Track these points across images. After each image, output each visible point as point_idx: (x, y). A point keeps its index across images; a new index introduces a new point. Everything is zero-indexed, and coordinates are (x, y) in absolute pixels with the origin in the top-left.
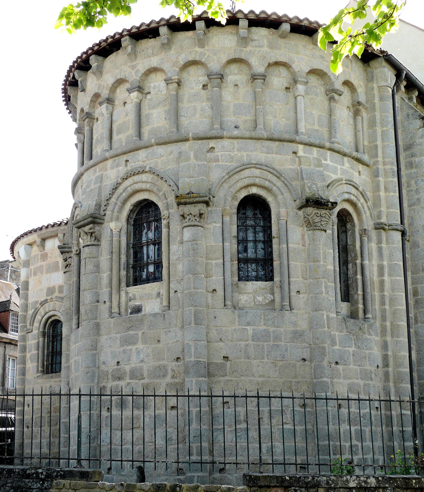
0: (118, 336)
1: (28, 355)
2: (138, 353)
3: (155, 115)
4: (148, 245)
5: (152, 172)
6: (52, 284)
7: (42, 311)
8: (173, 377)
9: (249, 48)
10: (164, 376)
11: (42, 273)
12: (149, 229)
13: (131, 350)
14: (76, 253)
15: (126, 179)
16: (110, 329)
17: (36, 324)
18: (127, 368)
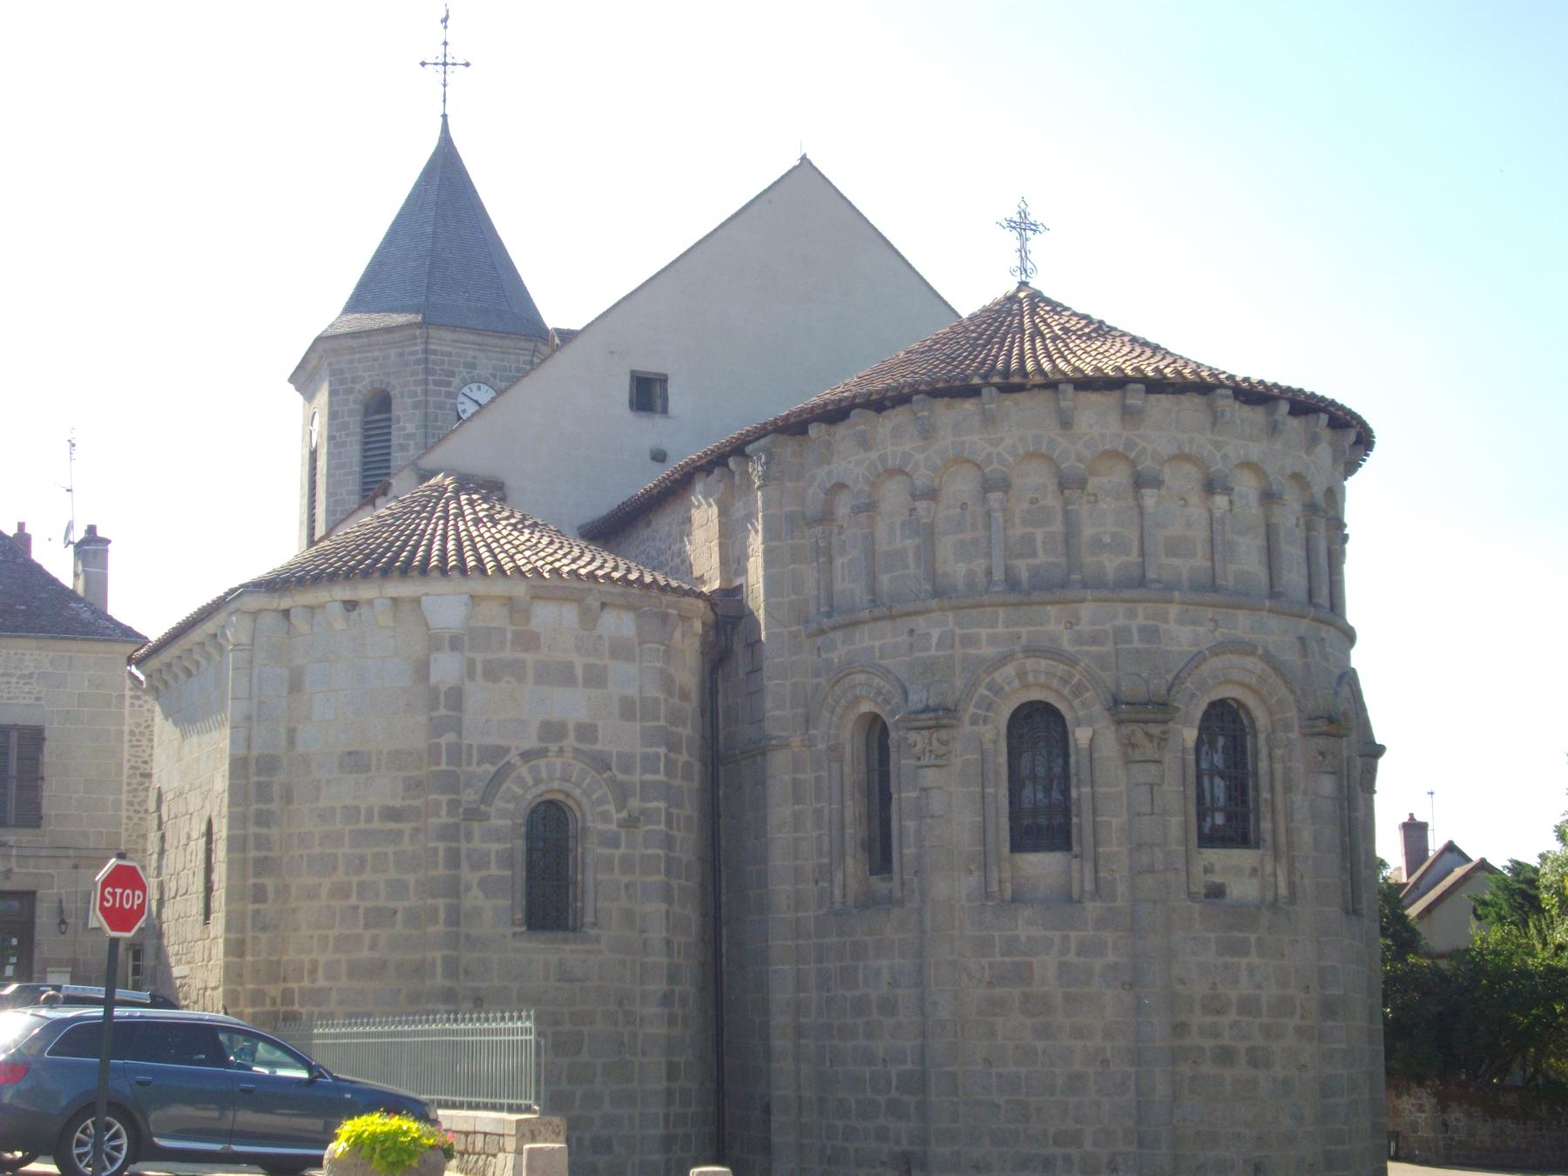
0: (1212, 935)
2: (1252, 971)
5: (1268, 658)
8: (1302, 1017)
10: (1292, 1014)
18: (1233, 995)
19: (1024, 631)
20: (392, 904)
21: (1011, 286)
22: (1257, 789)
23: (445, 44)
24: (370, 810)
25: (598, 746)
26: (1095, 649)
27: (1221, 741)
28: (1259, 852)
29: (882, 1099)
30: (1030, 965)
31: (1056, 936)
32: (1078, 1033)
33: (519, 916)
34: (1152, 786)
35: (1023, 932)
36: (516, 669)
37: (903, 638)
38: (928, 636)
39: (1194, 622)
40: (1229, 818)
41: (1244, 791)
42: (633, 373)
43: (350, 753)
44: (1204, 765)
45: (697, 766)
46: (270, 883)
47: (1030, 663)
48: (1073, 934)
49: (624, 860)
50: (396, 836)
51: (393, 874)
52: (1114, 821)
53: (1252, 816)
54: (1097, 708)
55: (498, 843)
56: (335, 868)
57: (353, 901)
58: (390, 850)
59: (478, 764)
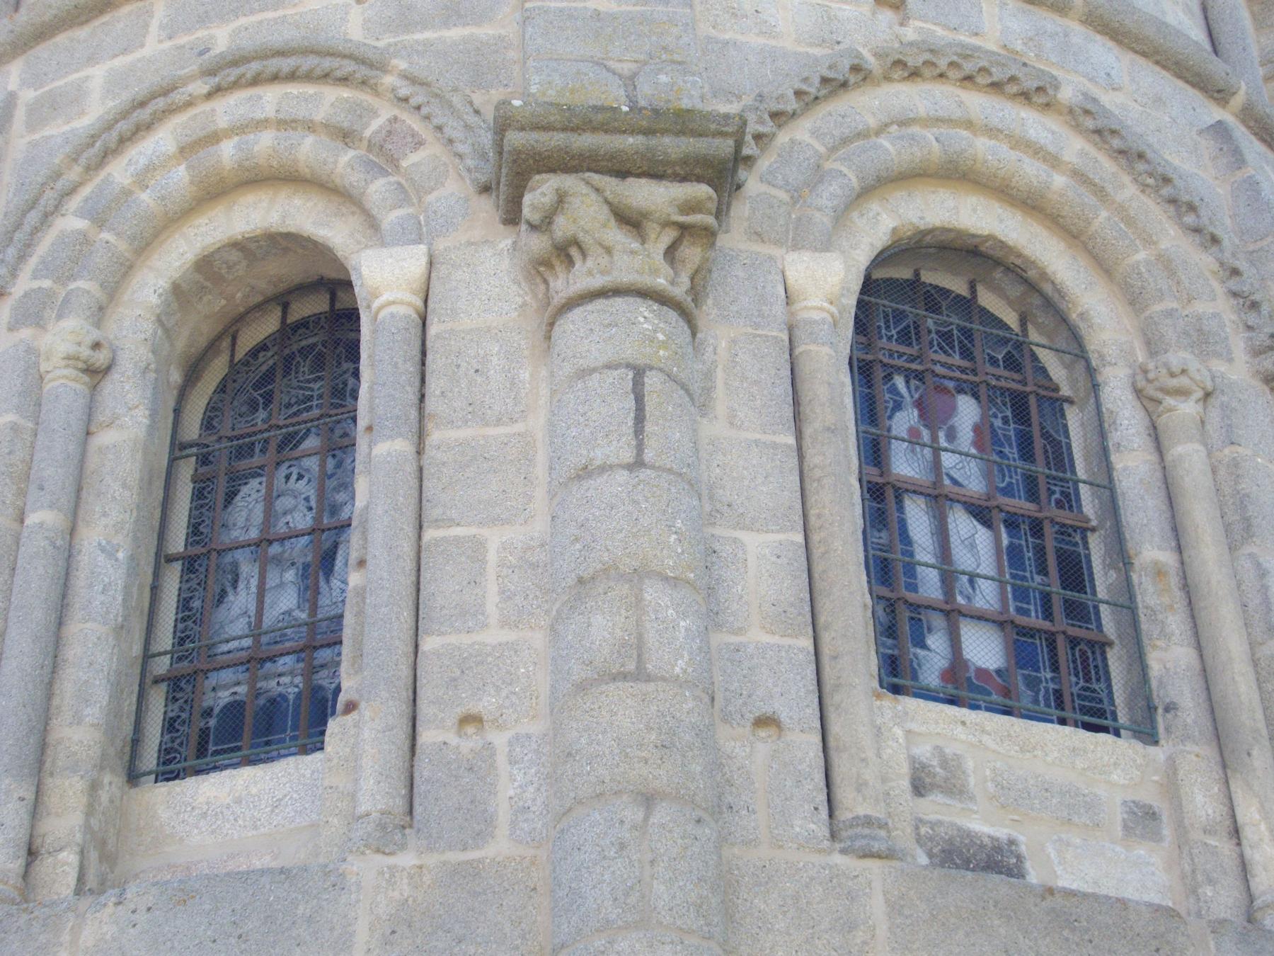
12: (934, 416)
14: (85, 352)
15: (914, 74)
16: (860, 936)
22: (1121, 557)
26: (455, 33)
27: (967, 412)
28: (1158, 754)
34: (639, 373)
41: (1074, 573)
44: (905, 465)
47: (229, 109)
52: (495, 539)
53: (1097, 549)
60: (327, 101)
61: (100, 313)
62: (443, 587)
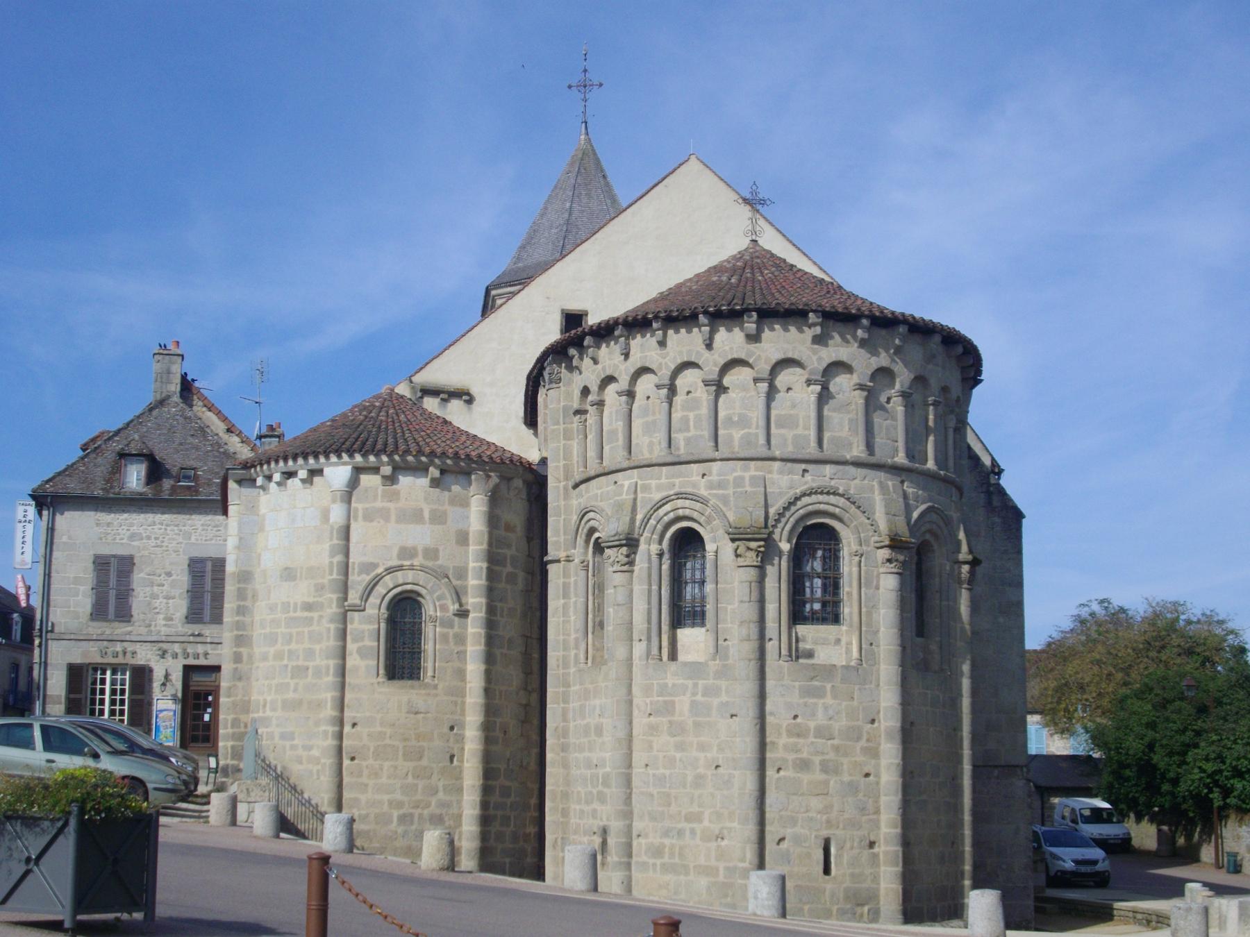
0: (797, 684)
1: (351, 646)
2: (826, 708)
3: (836, 421)
4: (811, 578)
6: (410, 543)
7: (388, 581)
8: (868, 740)
9: (930, 367)
10: (859, 739)
11: (387, 519)
12: (814, 558)
13: (816, 704)
17: (374, 600)
18: (812, 724)
19: (677, 481)
20: (307, 663)
21: (744, 243)
23: (585, 71)
24: (296, 604)
25: (439, 562)
26: (721, 492)
29: (595, 791)
30: (673, 703)
31: (690, 683)
32: (702, 747)
33: (382, 671)
35: (670, 681)
36: (384, 515)
37: (612, 487)
38: (622, 486)
39: (791, 472)
40: (824, 604)
42: (563, 311)
43: (286, 569)
45: (521, 575)
46: (244, 650)
47: (680, 503)
48: (701, 682)
49: (456, 636)
50: (309, 621)
51: (307, 645)
52: (730, 607)
54: (721, 532)
55: (368, 628)
56: (276, 641)
57: (285, 662)
58: (306, 630)
59: (360, 573)
60: (698, 506)
61: (660, 542)
62: (721, 616)
